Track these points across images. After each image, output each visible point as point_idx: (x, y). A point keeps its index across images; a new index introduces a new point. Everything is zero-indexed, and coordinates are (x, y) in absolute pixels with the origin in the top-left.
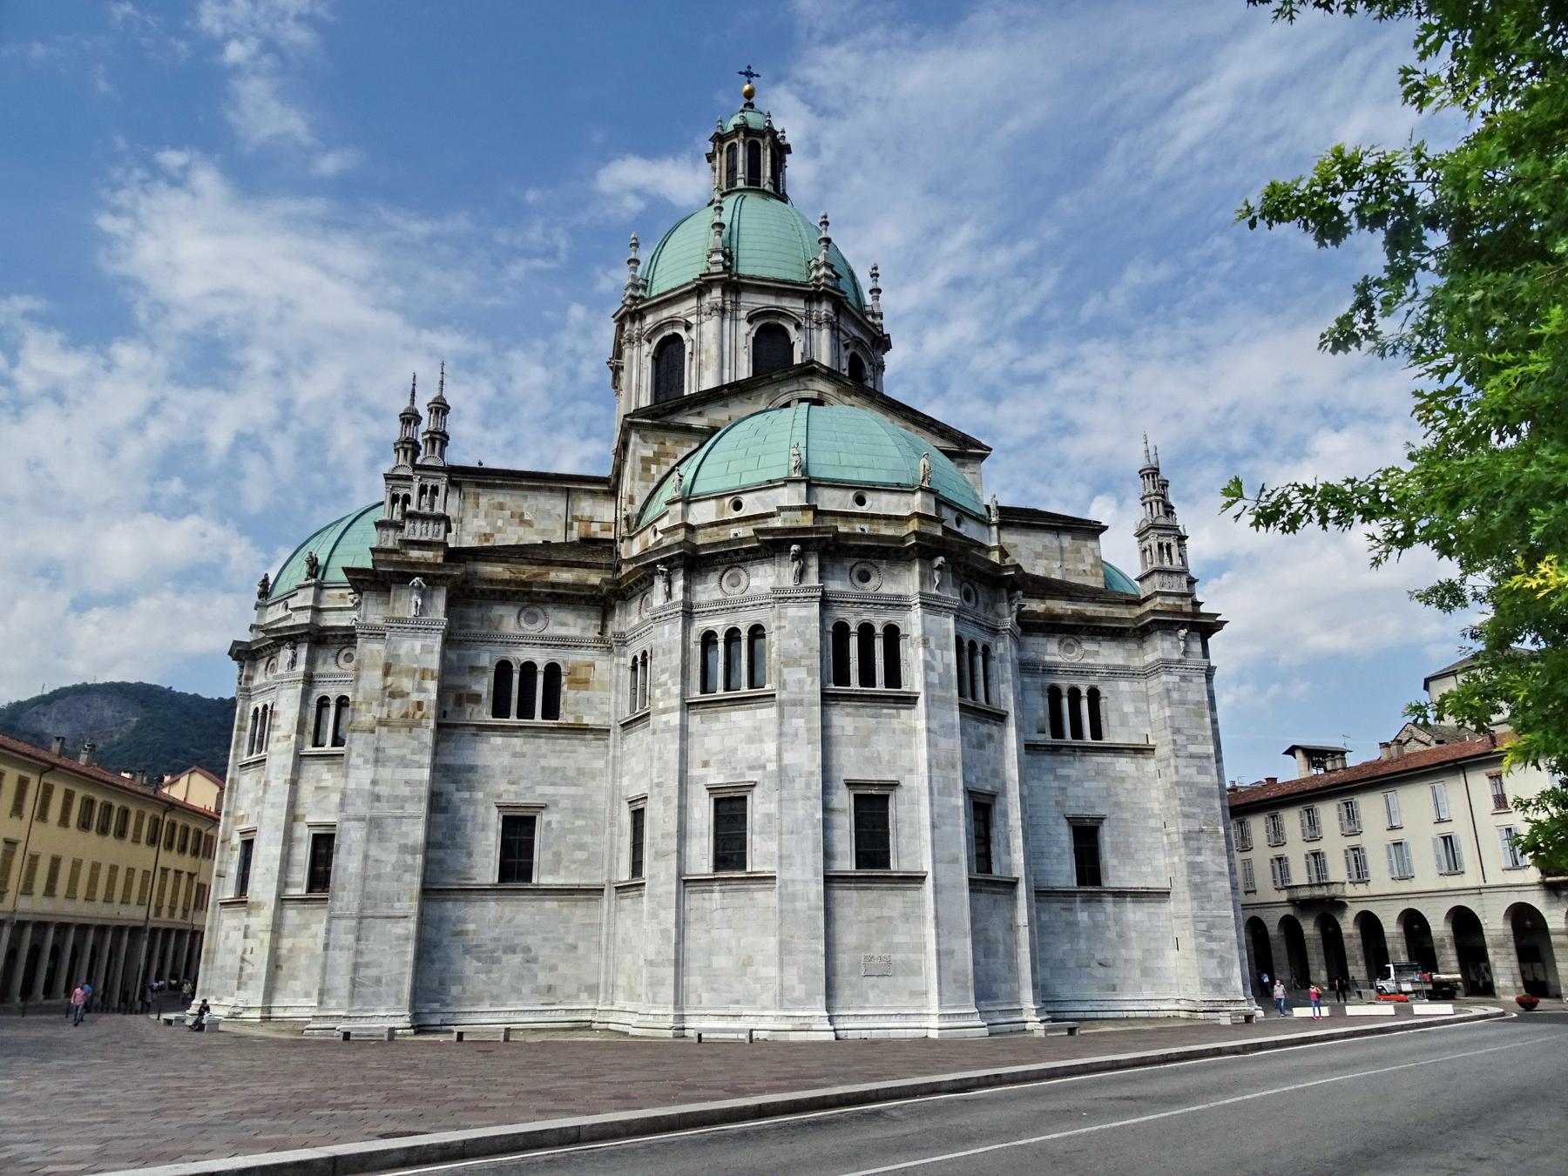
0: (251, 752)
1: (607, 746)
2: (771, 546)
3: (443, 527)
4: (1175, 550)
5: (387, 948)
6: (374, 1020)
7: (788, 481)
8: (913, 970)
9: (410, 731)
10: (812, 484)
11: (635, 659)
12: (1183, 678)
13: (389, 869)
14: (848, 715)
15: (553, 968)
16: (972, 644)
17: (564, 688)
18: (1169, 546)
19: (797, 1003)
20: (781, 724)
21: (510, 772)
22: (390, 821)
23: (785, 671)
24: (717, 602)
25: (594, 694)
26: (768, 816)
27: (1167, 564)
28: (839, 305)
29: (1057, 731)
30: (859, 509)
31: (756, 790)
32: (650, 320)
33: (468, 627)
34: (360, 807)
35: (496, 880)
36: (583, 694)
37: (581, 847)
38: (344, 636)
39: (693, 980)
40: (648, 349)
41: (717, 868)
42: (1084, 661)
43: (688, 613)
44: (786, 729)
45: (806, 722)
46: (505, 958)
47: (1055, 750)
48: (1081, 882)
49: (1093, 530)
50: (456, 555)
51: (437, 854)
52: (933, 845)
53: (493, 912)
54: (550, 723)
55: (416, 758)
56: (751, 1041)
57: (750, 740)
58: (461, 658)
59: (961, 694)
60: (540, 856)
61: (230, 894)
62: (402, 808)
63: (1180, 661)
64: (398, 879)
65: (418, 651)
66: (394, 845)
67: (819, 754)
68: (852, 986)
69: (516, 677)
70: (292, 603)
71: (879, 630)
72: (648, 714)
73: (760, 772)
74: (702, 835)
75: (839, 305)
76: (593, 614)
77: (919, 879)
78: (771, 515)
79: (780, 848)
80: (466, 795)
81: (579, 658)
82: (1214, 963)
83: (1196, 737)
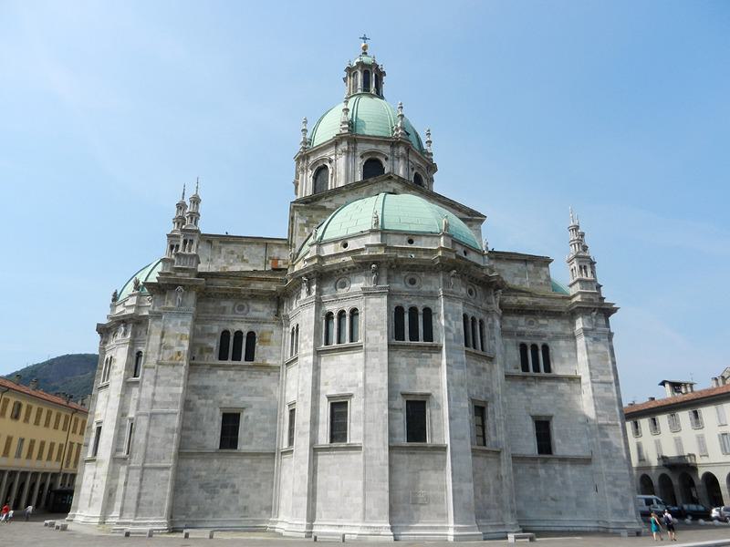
0: (103, 381)
2: (363, 265)
3: (195, 261)
4: (589, 270)
7: (372, 231)
8: (442, 500)
10: (384, 232)
12: (595, 339)
13: (159, 441)
14: (404, 356)
15: (247, 497)
16: (473, 319)
17: (257, 344)
18: (585, 267)
19: (373, 518)
20: (365, 361)
21: (227, 389)
22: (161, 417)
23: (368, 333)
25: (274, 348)
26: (358, 412)
27: (584, 277)
28: (409, 149)
29: (525, 368)
30: (409, 246)
32: (312, 160)
33: (208, 313)
34: (145, 409)
35: (218, 447)
36: (267, 348)
37: (264, 430)
39: (319, 504)
40: (311, 173)
41: (331, 442)
42: (539, 330)
43: (319, 303)
44: (367, 364)
45: (380, 359)
46: (221, 491)
47: (524, 378)
48: (540, 452)
49: (546, 261)
50: (200, 275)
51: (186, 433)
52: (450, 430)
54: (250, 363)
56: (344, 541)
57: (350, 371)
58: (203, 329)
59: (466, 345)
60: (242, 435)
61: (89, 455)
63: (592, 330)
64: (164, 447)
67: (386, 378)
68: (405, 509)
69: (232, 338)
70: (127, 304)
71: (420, 311)
74: (324, 423)
75: (409, 149)
76: (273, 306)
77: (443, 449)
78: (362, 250)
79: (364, 428)
80: (203, 401)
82: (618, 500)
83: (603, 371)
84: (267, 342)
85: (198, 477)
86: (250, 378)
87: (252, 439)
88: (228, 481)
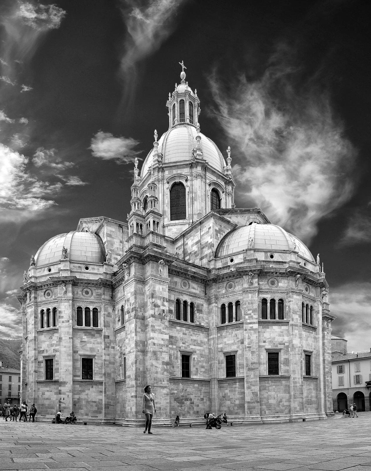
1: (208, 334)
11: (223, 306)
13: (160, 370)
17: (196, 312)
21: (183, 340)
22: (159, 353)
24: (269, 289)
25: (205, 316)
31: (282, 351)
35: (181, 376)
36: (201, 315)
37: (203, 367)
38: (85, 283)
53: (181, 387)
54: (192, 324)
55: (164, 331)
57: (280, 336)
60: (192, 369)
62: (162, 348)
66: (160, 362)
69: (182, 306)
74: (264, 364)
76: (202, 286)
80: (171, 346)
81: (199, 302)
84: (200, 311)
85: (173, 394)
86: (194, 334)
87: (197, 372)
88: (188, 397)
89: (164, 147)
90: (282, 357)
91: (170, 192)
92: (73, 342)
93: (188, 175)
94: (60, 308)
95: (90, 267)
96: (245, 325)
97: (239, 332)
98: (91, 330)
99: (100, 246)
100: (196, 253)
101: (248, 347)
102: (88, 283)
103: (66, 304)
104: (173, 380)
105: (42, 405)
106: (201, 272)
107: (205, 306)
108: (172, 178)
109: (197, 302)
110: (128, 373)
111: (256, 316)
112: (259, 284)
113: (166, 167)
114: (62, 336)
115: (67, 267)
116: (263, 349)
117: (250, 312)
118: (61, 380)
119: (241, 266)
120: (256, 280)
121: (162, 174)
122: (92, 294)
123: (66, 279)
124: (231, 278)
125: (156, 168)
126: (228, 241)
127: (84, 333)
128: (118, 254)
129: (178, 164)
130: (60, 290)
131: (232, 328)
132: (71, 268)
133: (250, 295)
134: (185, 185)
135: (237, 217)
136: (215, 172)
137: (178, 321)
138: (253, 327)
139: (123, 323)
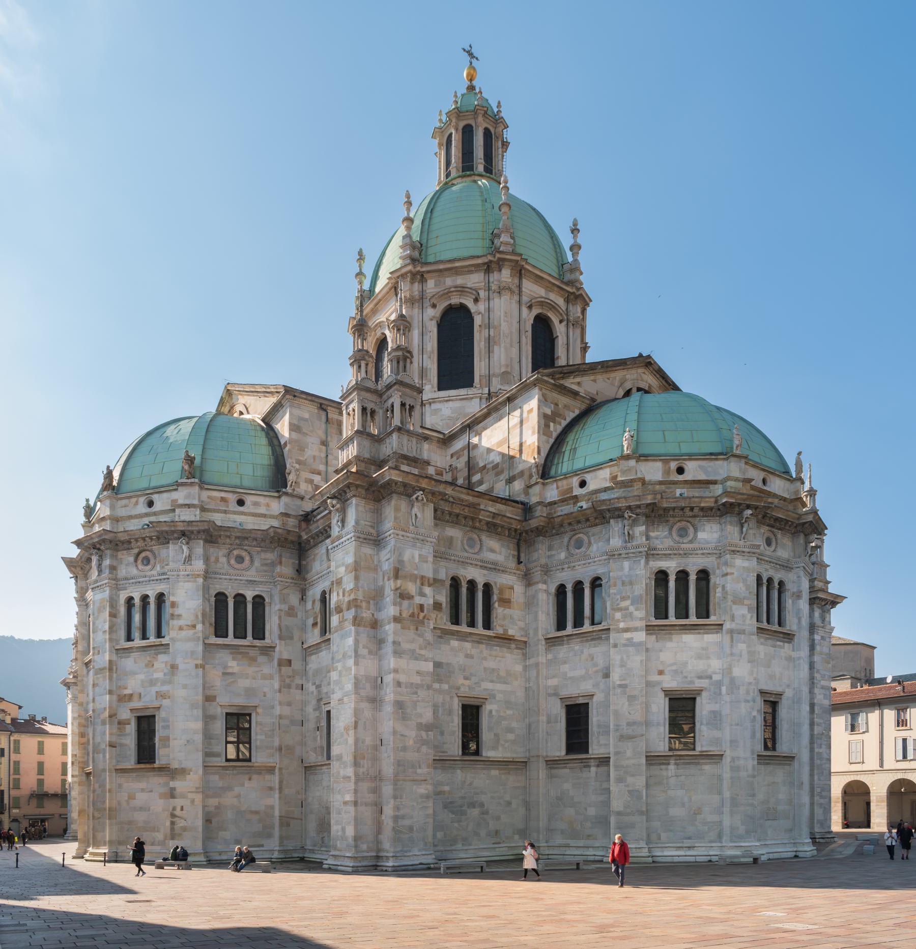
5: (415, 804)
6: (412, 858)
9: (417, 629)
11: (561, 590)
14: (762, 644)
17: (496, 605)
21: (464, 670)
31: (704, 694)
36: (507, 611)
38: (238, 538)
55: (423, 652)
57: (699, 657)
64: (418, 751)
65: (417, 560)
69: (464, 591)
72: (609, 629)
73: (707, 681)
76: (511, 546)
80: (436, 686)
81: (504, 582)
89: (426, 226)
90: (704, 708)
91: (439, 326)
92: (204, 676)
93: (480, 289)
94: (173, 595)
95: (249, 500)
96: (613, 636)
97: (597, 650)
98: (249, 646)
99: (274, 451)
100: (496, 466)
101: (620, 686)
102: (244, 537)
103: (189, 585)
104: (441, 762)
105: (130, 823)
106: (509, 512)
107: (519, 589)
108: (442, 295)
109: (500, 580)
110: (335, 750)
111: (640, 614)
112: (648, 538)
113: (429, 272)
114: (179, 661)
115: (195, 498)
116: (658, 689)
117: (627, 603)
118: (174, 765)
119: (604, 496)
120: (640, 529)
121: (421, 286)
122: (252, 561)
123: (190, 528)
124: (580, 525)
125: (406, 273)
126: (572, 438)
127: (231, 653)
128: (315, 470)
129: (457, 264)
130: (174, 552)
131: (582, 642)
132: (202, 502)
133: (626, 564)
134: (472, 311)
135: (594, 381)
136: (542, 278)
137: (455, 628)
138: (632, 638)
139: (324, 631)
